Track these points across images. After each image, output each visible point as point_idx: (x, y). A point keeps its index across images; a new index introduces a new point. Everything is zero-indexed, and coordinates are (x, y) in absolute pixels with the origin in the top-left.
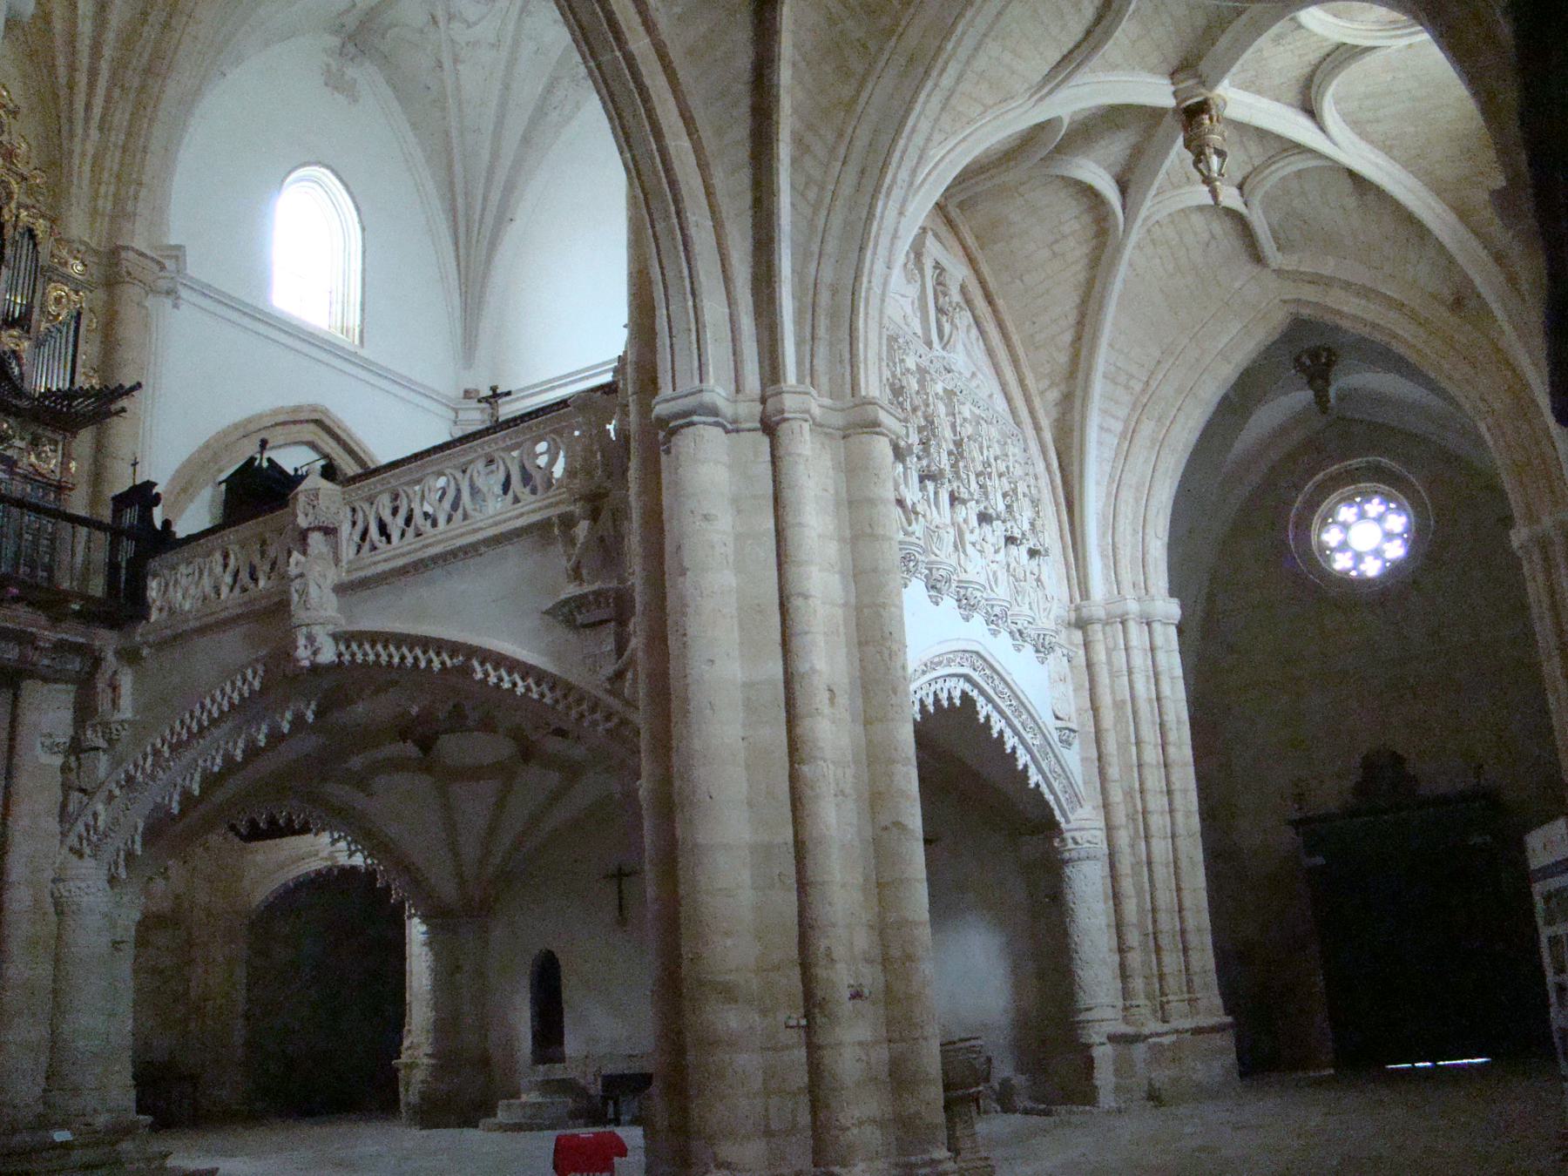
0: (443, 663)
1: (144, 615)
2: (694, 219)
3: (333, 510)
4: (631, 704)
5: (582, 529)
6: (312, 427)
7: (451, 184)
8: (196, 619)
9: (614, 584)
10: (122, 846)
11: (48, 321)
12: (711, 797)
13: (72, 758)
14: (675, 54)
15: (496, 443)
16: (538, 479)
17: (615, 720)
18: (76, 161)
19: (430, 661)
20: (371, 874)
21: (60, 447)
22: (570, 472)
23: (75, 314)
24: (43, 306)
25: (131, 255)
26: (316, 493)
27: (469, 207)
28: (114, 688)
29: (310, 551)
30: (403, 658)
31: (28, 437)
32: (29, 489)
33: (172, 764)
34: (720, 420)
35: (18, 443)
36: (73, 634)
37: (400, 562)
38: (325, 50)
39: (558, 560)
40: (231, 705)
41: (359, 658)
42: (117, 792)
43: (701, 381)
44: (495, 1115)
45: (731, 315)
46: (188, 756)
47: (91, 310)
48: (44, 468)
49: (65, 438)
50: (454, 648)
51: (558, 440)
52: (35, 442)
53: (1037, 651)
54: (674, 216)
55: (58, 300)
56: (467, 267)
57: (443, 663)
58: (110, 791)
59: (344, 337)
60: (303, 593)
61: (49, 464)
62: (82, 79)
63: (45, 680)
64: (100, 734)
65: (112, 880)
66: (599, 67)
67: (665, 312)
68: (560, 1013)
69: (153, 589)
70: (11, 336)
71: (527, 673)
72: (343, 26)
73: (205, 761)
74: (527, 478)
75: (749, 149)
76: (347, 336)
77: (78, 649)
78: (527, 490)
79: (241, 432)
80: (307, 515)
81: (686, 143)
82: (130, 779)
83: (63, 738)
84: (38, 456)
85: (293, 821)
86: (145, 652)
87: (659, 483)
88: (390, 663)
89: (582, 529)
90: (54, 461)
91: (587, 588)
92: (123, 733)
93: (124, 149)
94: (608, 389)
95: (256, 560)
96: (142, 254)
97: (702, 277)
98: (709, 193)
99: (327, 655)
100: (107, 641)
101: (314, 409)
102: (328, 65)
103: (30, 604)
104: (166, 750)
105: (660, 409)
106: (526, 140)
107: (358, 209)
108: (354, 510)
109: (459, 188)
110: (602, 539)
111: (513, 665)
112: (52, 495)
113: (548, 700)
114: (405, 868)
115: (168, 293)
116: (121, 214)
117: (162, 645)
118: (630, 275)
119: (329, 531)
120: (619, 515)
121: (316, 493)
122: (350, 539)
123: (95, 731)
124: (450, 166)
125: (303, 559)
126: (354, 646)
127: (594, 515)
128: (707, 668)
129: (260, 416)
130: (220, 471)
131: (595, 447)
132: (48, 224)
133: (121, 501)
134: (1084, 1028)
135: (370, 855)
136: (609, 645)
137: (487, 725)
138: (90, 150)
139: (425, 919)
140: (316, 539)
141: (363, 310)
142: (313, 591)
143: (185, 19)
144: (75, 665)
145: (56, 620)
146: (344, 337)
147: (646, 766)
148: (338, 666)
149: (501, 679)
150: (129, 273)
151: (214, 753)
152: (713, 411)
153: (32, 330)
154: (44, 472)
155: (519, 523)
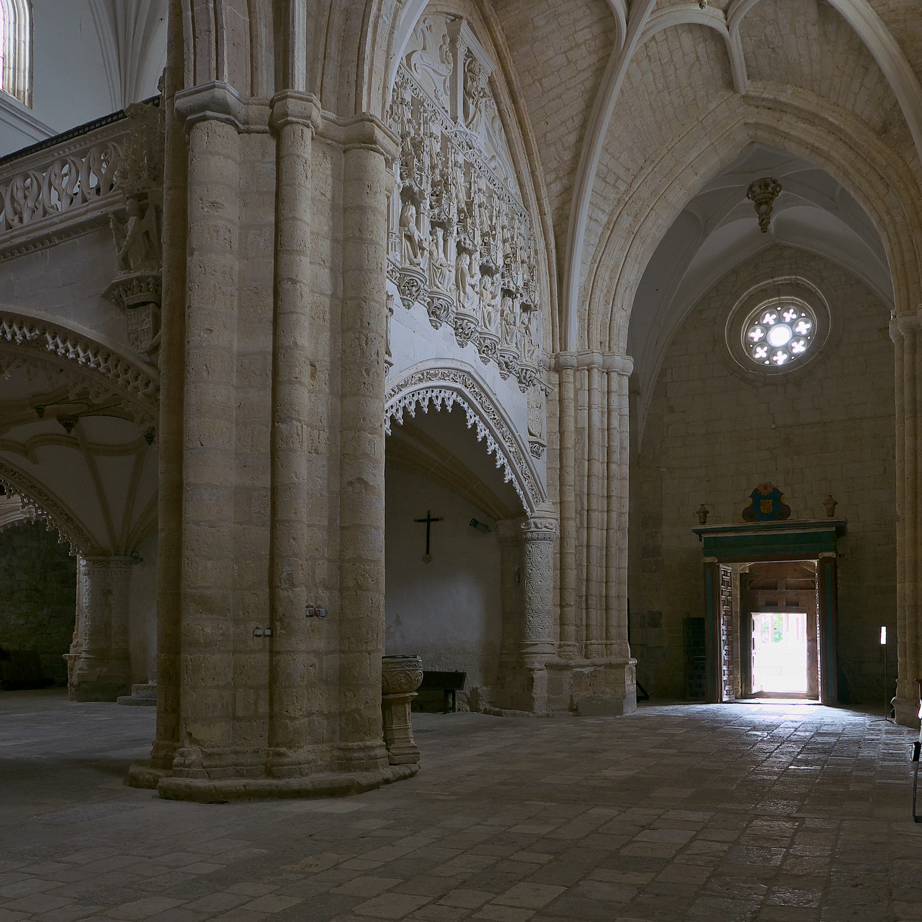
0: (24, 336)
17: (151, 385)
50: (33, 323)
53: (520, 382)
67: (190, 13)
105: (181, 103)
110: (147, 234)
127: (142, 213)
134: (528, 658)
136: (148, 325)
152: (223, 107)
155: (84, 218)
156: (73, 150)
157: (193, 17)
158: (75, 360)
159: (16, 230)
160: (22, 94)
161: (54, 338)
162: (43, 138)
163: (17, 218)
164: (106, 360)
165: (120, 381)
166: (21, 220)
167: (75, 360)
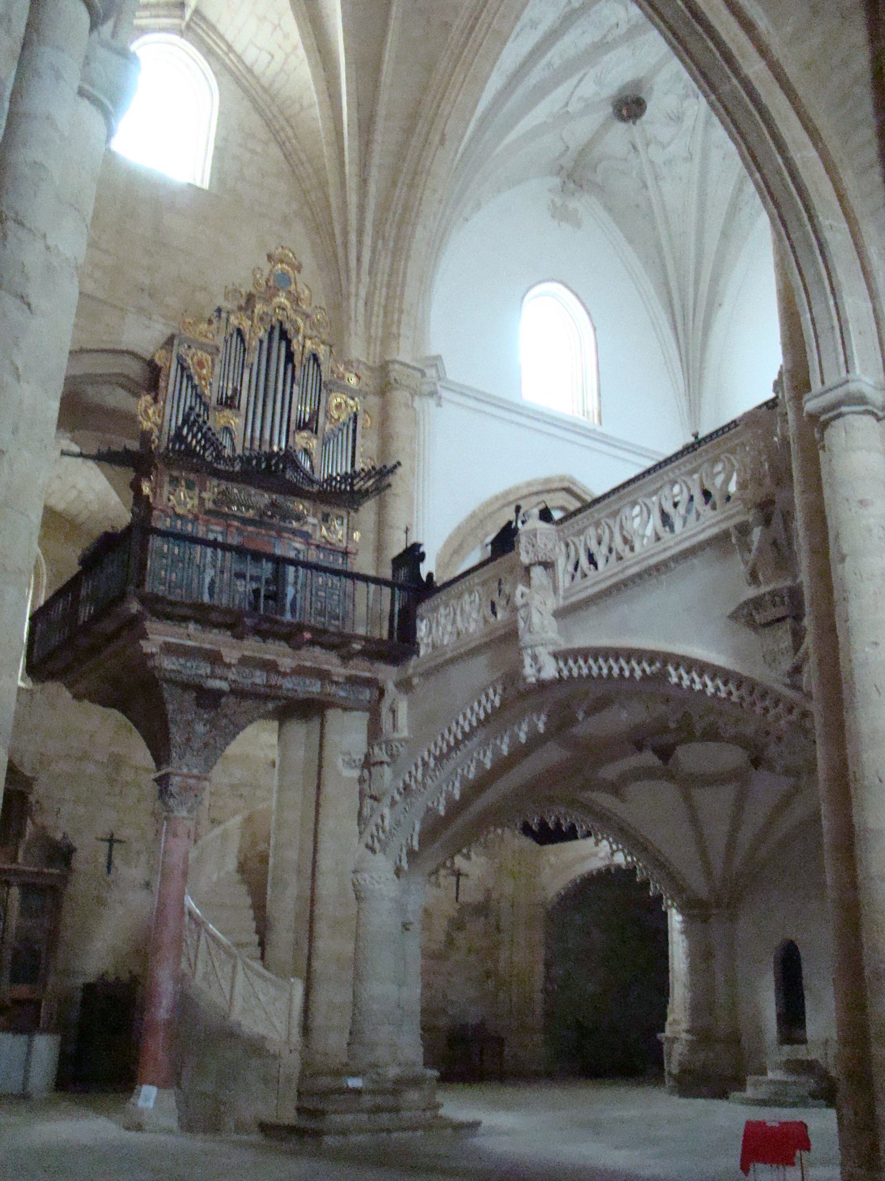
0: (644, 671)
1: (417, 652)
2: (827, 223)
3: (550, 546)
4: (809, 696)
5: (756, 534)
6: (563, 495)
7: (666, 284)
8: (452, 651)
9: (789, 583)
10: (404, 842)
11: (331, 423)
12: (880, 781)
13: (366, 772)
14: (791, 71)
15: (680, 469)
16: (716, 496)
17: (796, 712)
18: (353, 300)
19: (632, 670)
20: (631, 872)
21: (345, 521)
22: (742, 486)
23: (352, 415)
24: (327, 412)
25: (397, 366)
26: (534, 533)
27: (683, 299)
28: (394, 712)
29: (533, 582)
30: (610, 669)
31: (320, 516)
32: (322, 556)
33: (437, 773)
34: (870, 408)
35: (311, 520)
36: (361, 669)
37: (603, 586)
38: (550, 190)
39: (738, 567)
40: (478, 720)
41: (575, 673)
42: (397, 797)
43: (848, 371)
44: (745, 1091)
45: (874, 310)
46: (449, 765)
47: (365, 412)
48: (333, 539)
49: (349, 513)
50: (652, 657)
51: (732, 457)
52: (325, 518)
54: (807, 222)
55: (338, 406)
56: (687, 351)
57: (644, 671)
58: (393, 797)
59: (585, 419)
60: (528, 619)
61: (337, 535)
62: (353, 237)
63: (345, 709)
64: (384, 751)
65: (398, 872)
66: (719, 99)
67: (808, 316)
68: (801, 997)
69: (422, 629)
70: (302, 437)
71: (691, 667)
72: (562, 168)
73: (463, 770)
74: (707, 494)
75: (876, 149)
76: (588, 418)
77: (370, 683)
78: (708, 507)
79: (501, 502)
80: (528, 553)
81: (812, 153)
82: (406, 787)
83: (360, 757)
84: (328, 529)
85: (561, 825)
86: (415, 681)
87: (819, 479)
88: (600, 675)
89: (756, 534)
90: (341, 533)
91: (764, 589)
92: (401, 749)
93: (388, 286)
94: (771, 405)
95: (496, 597)
96: (408, 366)
97: (841, 274)
98: (841, 198)
99: (550, 671)
100: (388, 674)
101: (562, 479)
102: (552, 201)
103: (323, 646)
104: (432, 762)
105: (811, 405)
106: (725, 235)
107: (589, 313)
108: (567, 545)
109: (673, 284)
110: (775, 543)
111: (702, 668)
112: (340, 560)
113: (734, 698)
114: (660, 864)
115: (432, 394)
116: (389, 337)
117: (426, 675)
118: (779, 291)
119: (548, 565)
120: (788, 517)
121: (534, 533)
122: (565, 569)
123: (381, 749)
124: (664, 266)
125: (526, 590)
126: (571, 662)
127: (767, 521)
128: (871, 651)
129: (518, 488)
130: (486, 535)
131: (764, 457)
132: (328, 348)
133: (398, 562)
135: (631, 854)
136: (786, 641)
137: (712, 735)
138: (363, 293)
139: (681, 910)
140: (537, 573)
141: (599, 395)
142: (536, 618)
143: (424, 175)
144: (366, 695)
145: (346, 658)
146: (585, 419)
147: (820, 753)
148: (559, 681)
149: (693, 681)
150: (395, 380)
151: (469, 762)
152: (861, 400)
153: (319, 431)
154: (333, 541)
155: (702, 537)
156: (683, 469)
157: (813, 320)
158: (703, 692)
159: (629, 560)
160: (591, 414)
161: (676, 669)
162: (650, 464)
163: (627, 548)
164: (738, 688)
165: (758, 709)
166: (632, 549)
167: (703, 692)
